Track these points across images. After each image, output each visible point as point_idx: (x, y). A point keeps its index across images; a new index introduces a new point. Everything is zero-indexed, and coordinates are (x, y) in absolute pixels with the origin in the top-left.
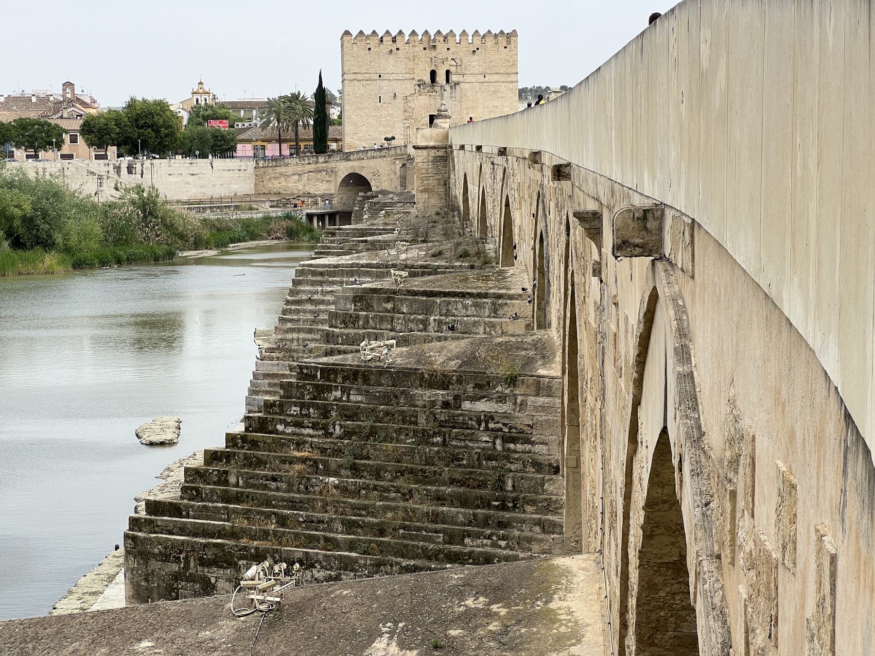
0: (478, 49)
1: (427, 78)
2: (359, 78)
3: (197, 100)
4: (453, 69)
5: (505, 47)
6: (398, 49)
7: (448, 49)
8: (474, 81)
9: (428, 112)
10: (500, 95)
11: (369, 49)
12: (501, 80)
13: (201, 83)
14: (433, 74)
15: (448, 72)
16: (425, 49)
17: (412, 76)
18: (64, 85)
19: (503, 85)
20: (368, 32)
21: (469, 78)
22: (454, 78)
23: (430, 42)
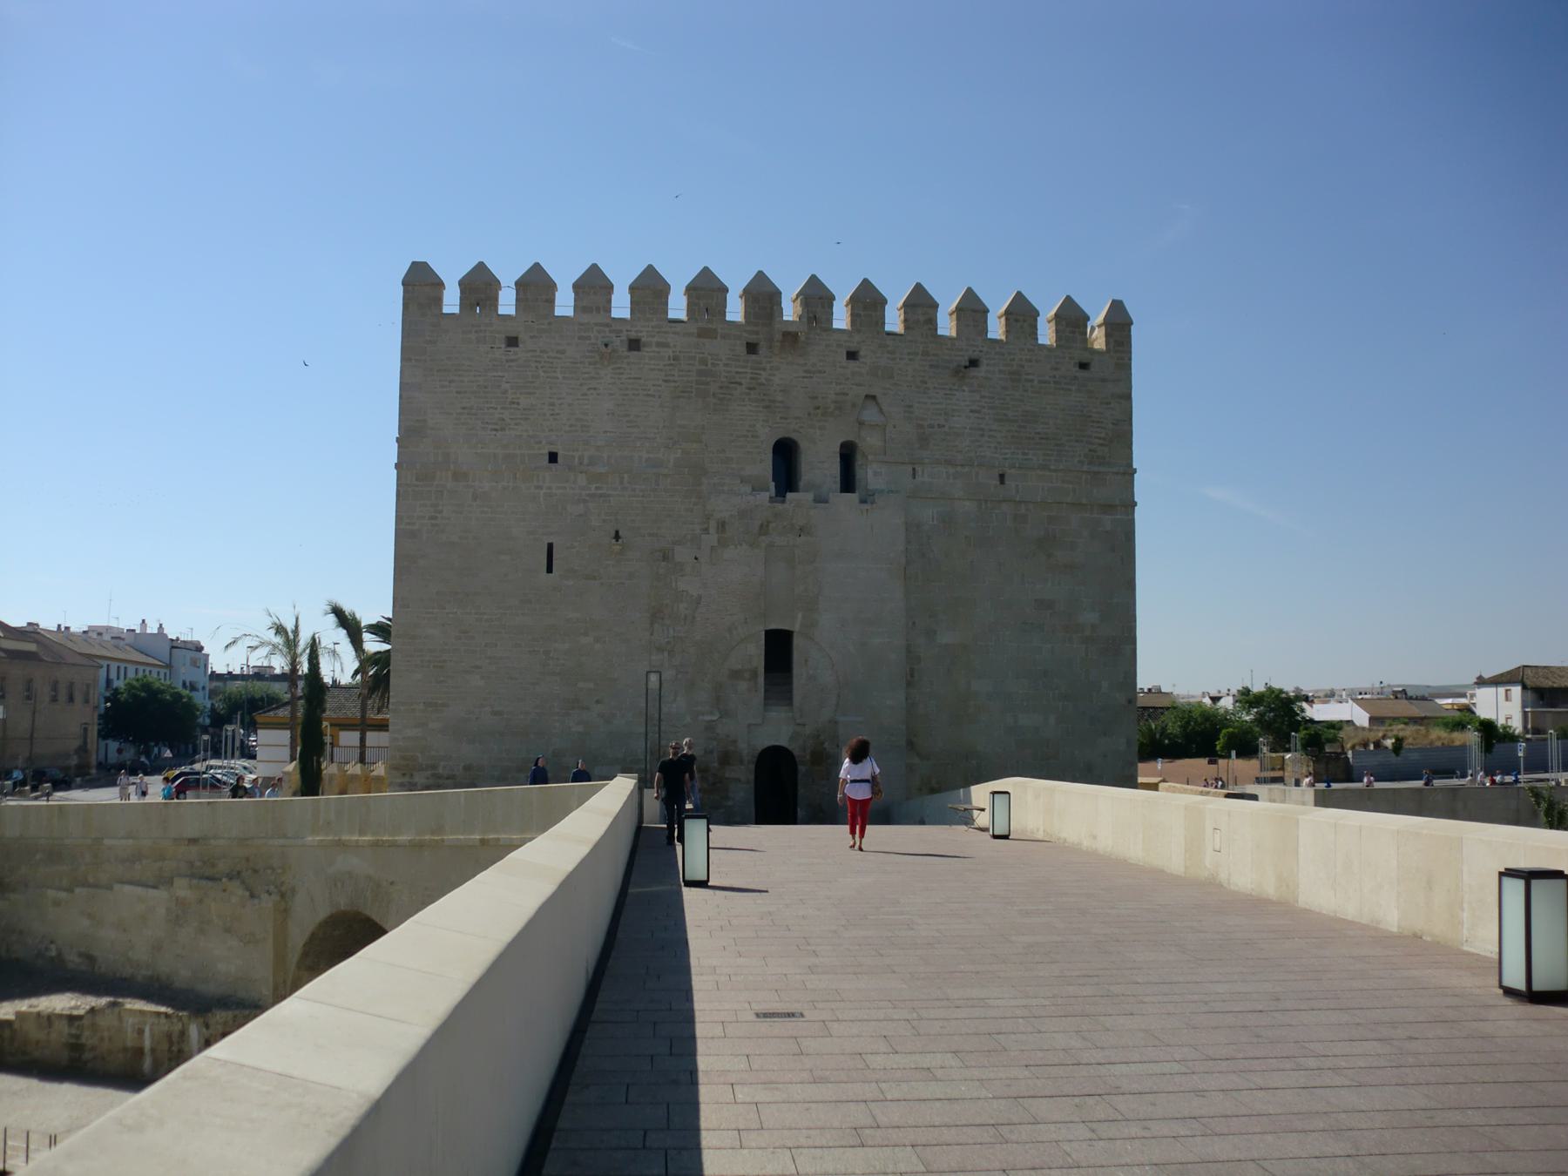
1: (763, 466)
4: (869, 442)
5: (1084, 366)
6: (634, 345)
7: (852, 355)
15: (848, 455)
16: (752, 348)
22: (870, 474)
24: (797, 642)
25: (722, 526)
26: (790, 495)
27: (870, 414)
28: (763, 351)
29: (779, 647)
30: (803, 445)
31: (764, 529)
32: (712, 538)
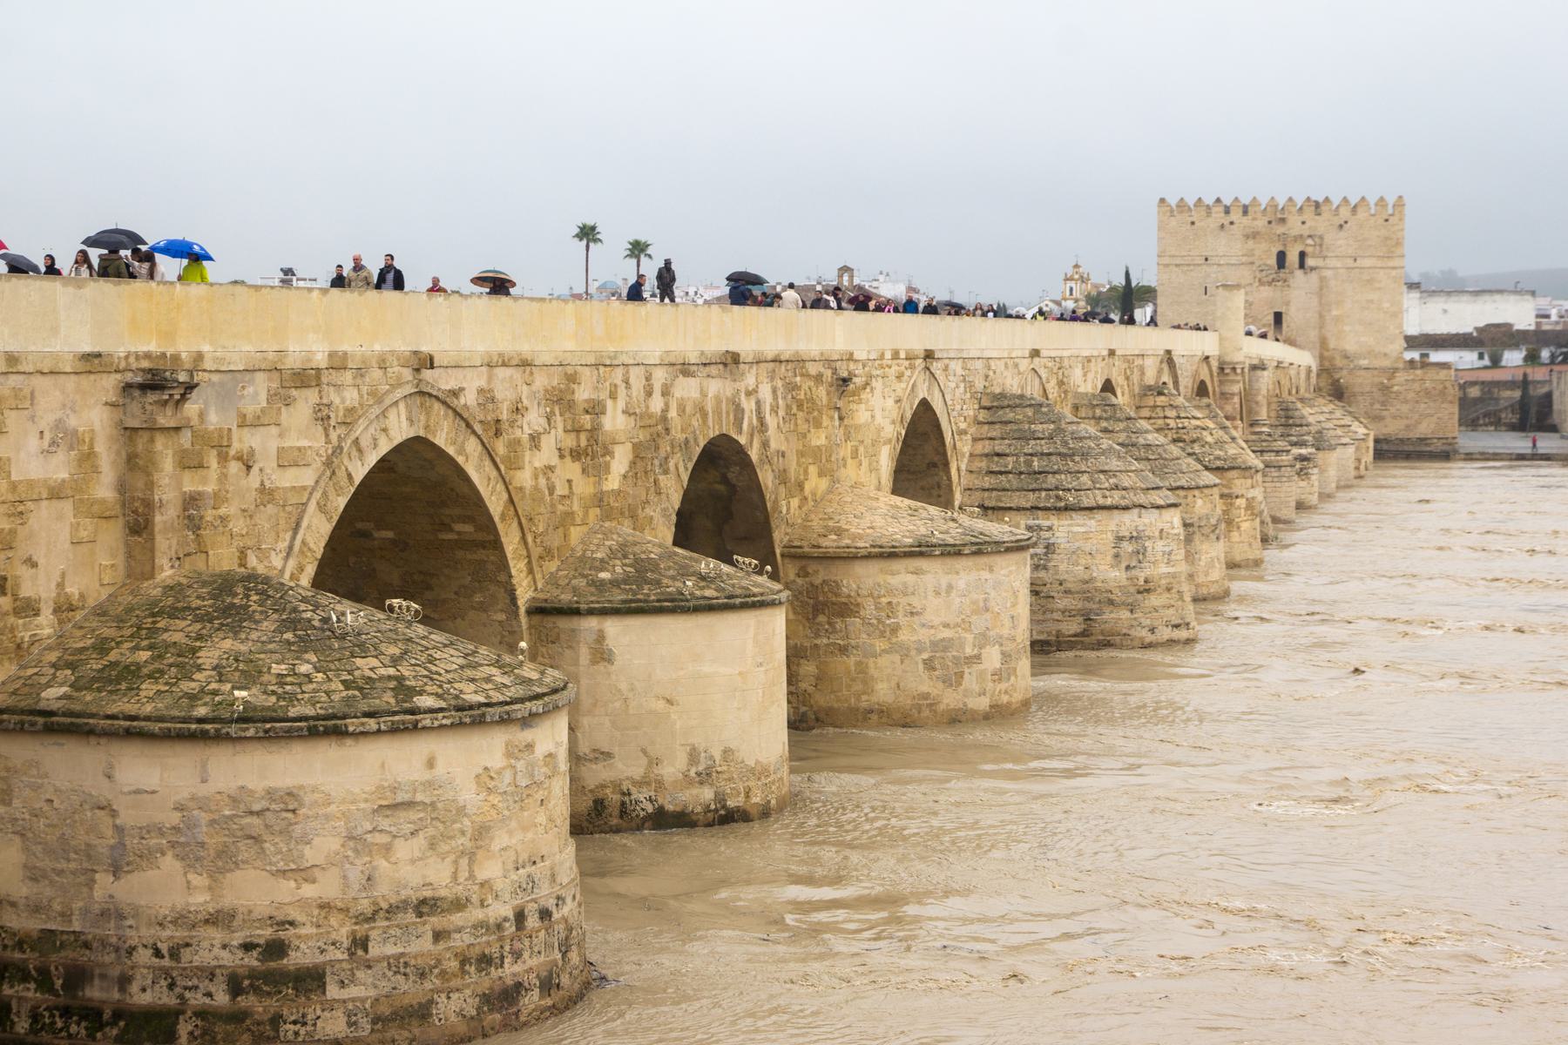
0: (1346, 222)
1: (1273, 261)
2: (1178, 262)
3: (1071, 289)
4: (1309, 250)
5: (1387, 220)
6: (1232, 223)
7: (1303, 223)
8: (1339, 266)
9: (1272, 308)
10: (1377, 285)
11: (1193, 223)
12: (1380, 265)
13: (1076, 266)
14: (1281, 258)
15: (1302, 255)
16: (1270, 222)
17: (1250, 259)
18: (840, 269)
19: (1382, 272)
20: (1191, 201)
21: (1331, 262)
22: (1310, 262)
23: (1277, 215)
24: (1284, 316)
25: (1260, 280)
26: (1282, 270)
27: (1310, 241)
28: (1273, 223)
29: (1278, 318)
30: (1288, 253)
31: (1273, 280)
32: (1257, 284)
